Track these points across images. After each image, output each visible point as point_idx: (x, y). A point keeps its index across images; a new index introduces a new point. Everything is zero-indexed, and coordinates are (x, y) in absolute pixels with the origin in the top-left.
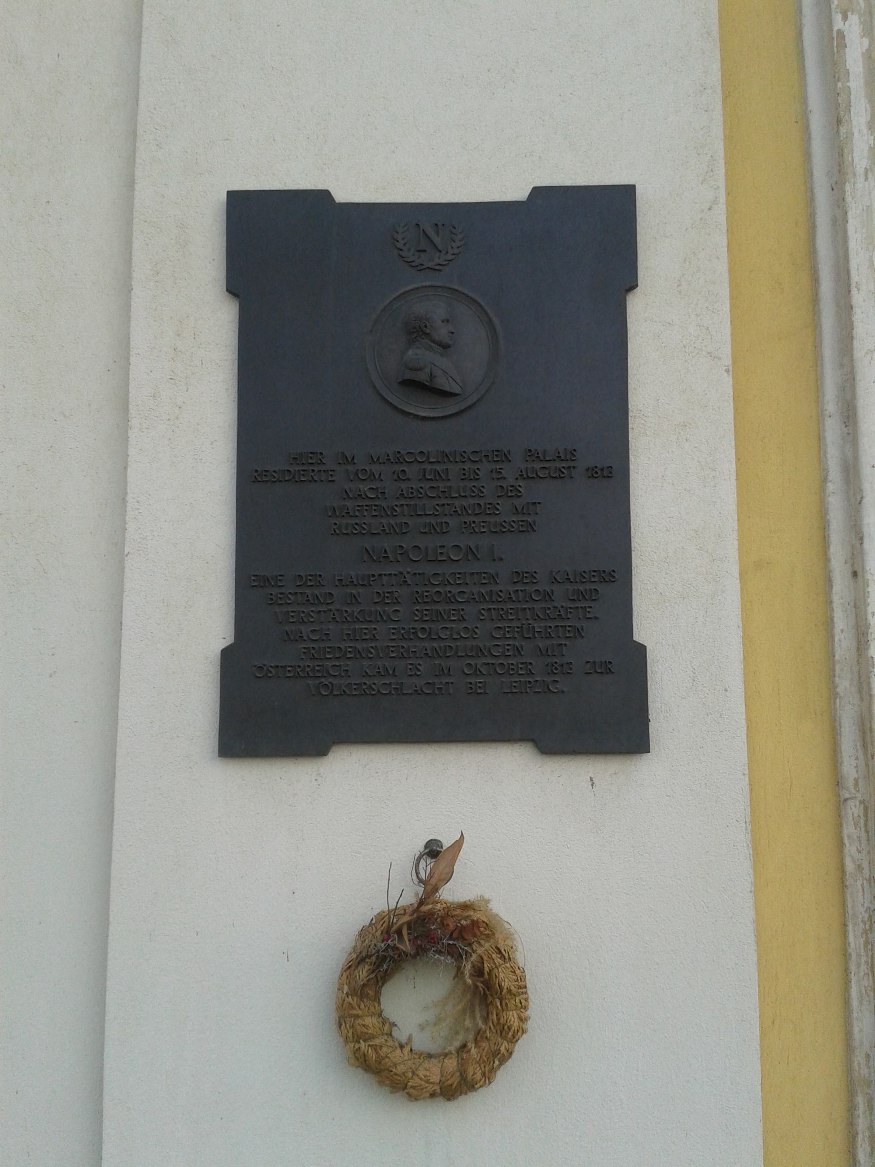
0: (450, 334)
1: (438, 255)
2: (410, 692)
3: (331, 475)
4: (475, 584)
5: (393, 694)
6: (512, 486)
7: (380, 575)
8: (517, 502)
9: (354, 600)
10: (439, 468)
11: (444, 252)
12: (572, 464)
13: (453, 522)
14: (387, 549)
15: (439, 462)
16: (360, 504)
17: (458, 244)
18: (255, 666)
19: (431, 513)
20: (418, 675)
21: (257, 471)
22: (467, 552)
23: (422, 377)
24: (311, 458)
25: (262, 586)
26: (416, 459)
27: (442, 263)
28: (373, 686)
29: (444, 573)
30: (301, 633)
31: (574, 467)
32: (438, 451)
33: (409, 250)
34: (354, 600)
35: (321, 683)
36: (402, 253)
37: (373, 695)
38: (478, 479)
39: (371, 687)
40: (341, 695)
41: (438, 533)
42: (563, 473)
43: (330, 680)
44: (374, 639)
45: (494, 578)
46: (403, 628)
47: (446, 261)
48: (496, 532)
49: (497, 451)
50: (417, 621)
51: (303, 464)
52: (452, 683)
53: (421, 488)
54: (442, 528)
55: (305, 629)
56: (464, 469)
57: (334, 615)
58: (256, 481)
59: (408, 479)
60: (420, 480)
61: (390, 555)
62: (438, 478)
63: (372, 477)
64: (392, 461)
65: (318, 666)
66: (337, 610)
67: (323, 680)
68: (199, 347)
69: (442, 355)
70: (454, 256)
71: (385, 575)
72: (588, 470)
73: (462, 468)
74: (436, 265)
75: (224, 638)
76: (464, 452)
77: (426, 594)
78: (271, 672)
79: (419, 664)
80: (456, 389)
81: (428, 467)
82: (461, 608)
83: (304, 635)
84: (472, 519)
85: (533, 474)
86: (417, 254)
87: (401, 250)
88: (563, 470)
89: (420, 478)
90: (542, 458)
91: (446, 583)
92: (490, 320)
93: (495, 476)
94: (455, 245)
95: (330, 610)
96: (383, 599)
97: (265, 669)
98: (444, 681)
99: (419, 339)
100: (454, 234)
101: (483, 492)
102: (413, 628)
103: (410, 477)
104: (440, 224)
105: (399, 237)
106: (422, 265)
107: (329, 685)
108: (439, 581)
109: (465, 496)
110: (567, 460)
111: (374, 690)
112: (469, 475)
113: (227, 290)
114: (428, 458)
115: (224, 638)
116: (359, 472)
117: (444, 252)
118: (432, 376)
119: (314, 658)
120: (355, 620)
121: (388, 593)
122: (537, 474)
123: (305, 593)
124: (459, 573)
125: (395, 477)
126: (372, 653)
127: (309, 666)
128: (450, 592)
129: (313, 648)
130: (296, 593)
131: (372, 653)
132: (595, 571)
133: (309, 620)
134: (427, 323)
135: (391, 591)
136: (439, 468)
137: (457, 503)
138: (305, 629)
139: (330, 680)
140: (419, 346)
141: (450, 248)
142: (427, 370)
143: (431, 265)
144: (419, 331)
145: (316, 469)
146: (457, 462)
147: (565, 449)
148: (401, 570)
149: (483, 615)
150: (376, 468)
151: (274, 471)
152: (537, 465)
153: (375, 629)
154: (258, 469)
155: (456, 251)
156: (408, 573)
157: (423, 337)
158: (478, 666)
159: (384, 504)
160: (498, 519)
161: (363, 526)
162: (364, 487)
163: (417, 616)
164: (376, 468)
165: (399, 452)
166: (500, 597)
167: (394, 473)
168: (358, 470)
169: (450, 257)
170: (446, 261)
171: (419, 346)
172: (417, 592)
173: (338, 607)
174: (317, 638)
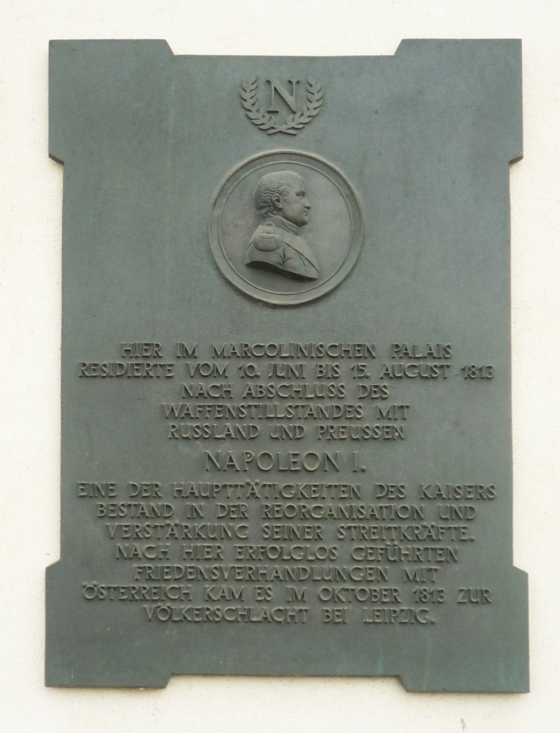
0: (306, 210)
1: (291, 116)
2: (259, 619)
3: (169, 371)
4: (333, 498)
5: (239, 621)
6: (376, 387)
7: (225, 486)
8: (382, 405)
9: (195, 514)
10: (292, 364)
11: (299, 114)
12: (444, 363)
13: (309, 427)
14: (233, 457)
15: (292, 357)
16: (202, 404)
17: (316, 105)
18: (84, 587)
19: (283, 415)
20: (268, 601)
21: (84, 365)
22: (324, 461)
23: (273, 259)
24: (146, 350)
25: (91, 497)
26: (266, 354)
27: (296, 127)
28: (217, 612)
29: (298, 485)
30: (136, 550)
31: (448, 366)
32: (290, 344)
33: (258, 111)
34: (195, 514)
35: (159, 607)
36: (251, 115)
37: (217, 622)
38: (337, 377)
39: (214, 612)
40: (181, 621)
41: (291, 439)
42: (435, 373)
43: (169, 604)
44: (218, 558)
45: (355, 494)
46: (251, 548)
47: (301, 123)
48: (357, 439)
49: (359, 345)
50: (265, 539)
51: (137, 357)
52: (306, 611)
53: (272, 386)
54: (295, 434)
55: (141, 547)
56: (321, 366)
57: (172, 530)
58: (83, 376)
59: (257, 376)
60: (270, 377)
61: (235, 463)
62: (290, 375)
63: (215, 373)
64: (238, 354)
65: (155, 588)
66: (176, 525)
67: (159, 604)
68: (18, 221)
69: (296, 234)
70: (311, 119)
71: (230, 486)
72: (463, 370)
73: (319, 364)
74: (289, 129)
75: (48, 554)
76: (321, 346)
77: (276, 509)
78: (102, 594)
79: (269, 589)
80: (312, 273)
81: (279, 362)
82: (316, 525)
83: (139, 552)
84: (330, 423)
85: (401, 372)
86: (268, 116)
87: (250, 111)
88: (435, 369)
89: (270, 375)
90: (411, 355)
91: (300, 496)
92: (352, 193)
93: (356, 374)
94: (311, 106)
95: (168, 525)
96: (228, 514)
97: (96, 589)
98: (297, 608)
99: (269, 214)
100: (310, 93)
101: (342, 393)
102: (262, 548)
103: (259, 374)
104: (294, 81)
105: (246, 96)
106: (273, 128)
107: (168, 609)
108: (291, 494)
109: (322, 397)
110: (440, 358)
111: (218, 616)
112: (327, 373)
113: (51, 156)
114: (280, 352)
115: (48, 554)
116: (200, 366)
117: (299, 114)
118: (284, 258)
119: (150, 579)
120: (196, 536)
121: (233, 506)
122: (405, 373)
123: (140, 505)
124: (315, 486)
125: (242, 374)
126: (215, 575)
127: (144, 588)
128: (304, 507)
129: (150, 568)
130: (130, 505)
131: (215, 575)
132: (470, 487)
133: (144, 535)
134: (280, 196)
135: (236, 504)
136: (292, 364)
137: (312, 404)
138: (141, 547)
139: (169, 604)
140: (271, 222)
141: (305, 109)
142: (280, 251)
143: (283, 128)
144: (270, 206)
145: (152, 364)
146: (313, 357)
147: (438, 345)
148: (248, 480)
149: (342, 534)
150: (221, 364)
151: (105, 365)
152: (406, 363)
153: (219, 547)
154: (87, 363)
155: (314, 113)
156: (257, 484)
157: (275, 212)
158: (336, 592)
159: (228, 405)
160: (359, 425)
161: (206, 429)
162: (205, 385)
163: (267, 533)
164: (221, 364)
165: (246, 346)
166: (362, 513)
167: (240, 369)
168: (199, 364)
169: (307, 120)
170: (301, 123)
171: (271, 222)
172: (267, 507)
173: (177, 522)
174: (153, 556)
